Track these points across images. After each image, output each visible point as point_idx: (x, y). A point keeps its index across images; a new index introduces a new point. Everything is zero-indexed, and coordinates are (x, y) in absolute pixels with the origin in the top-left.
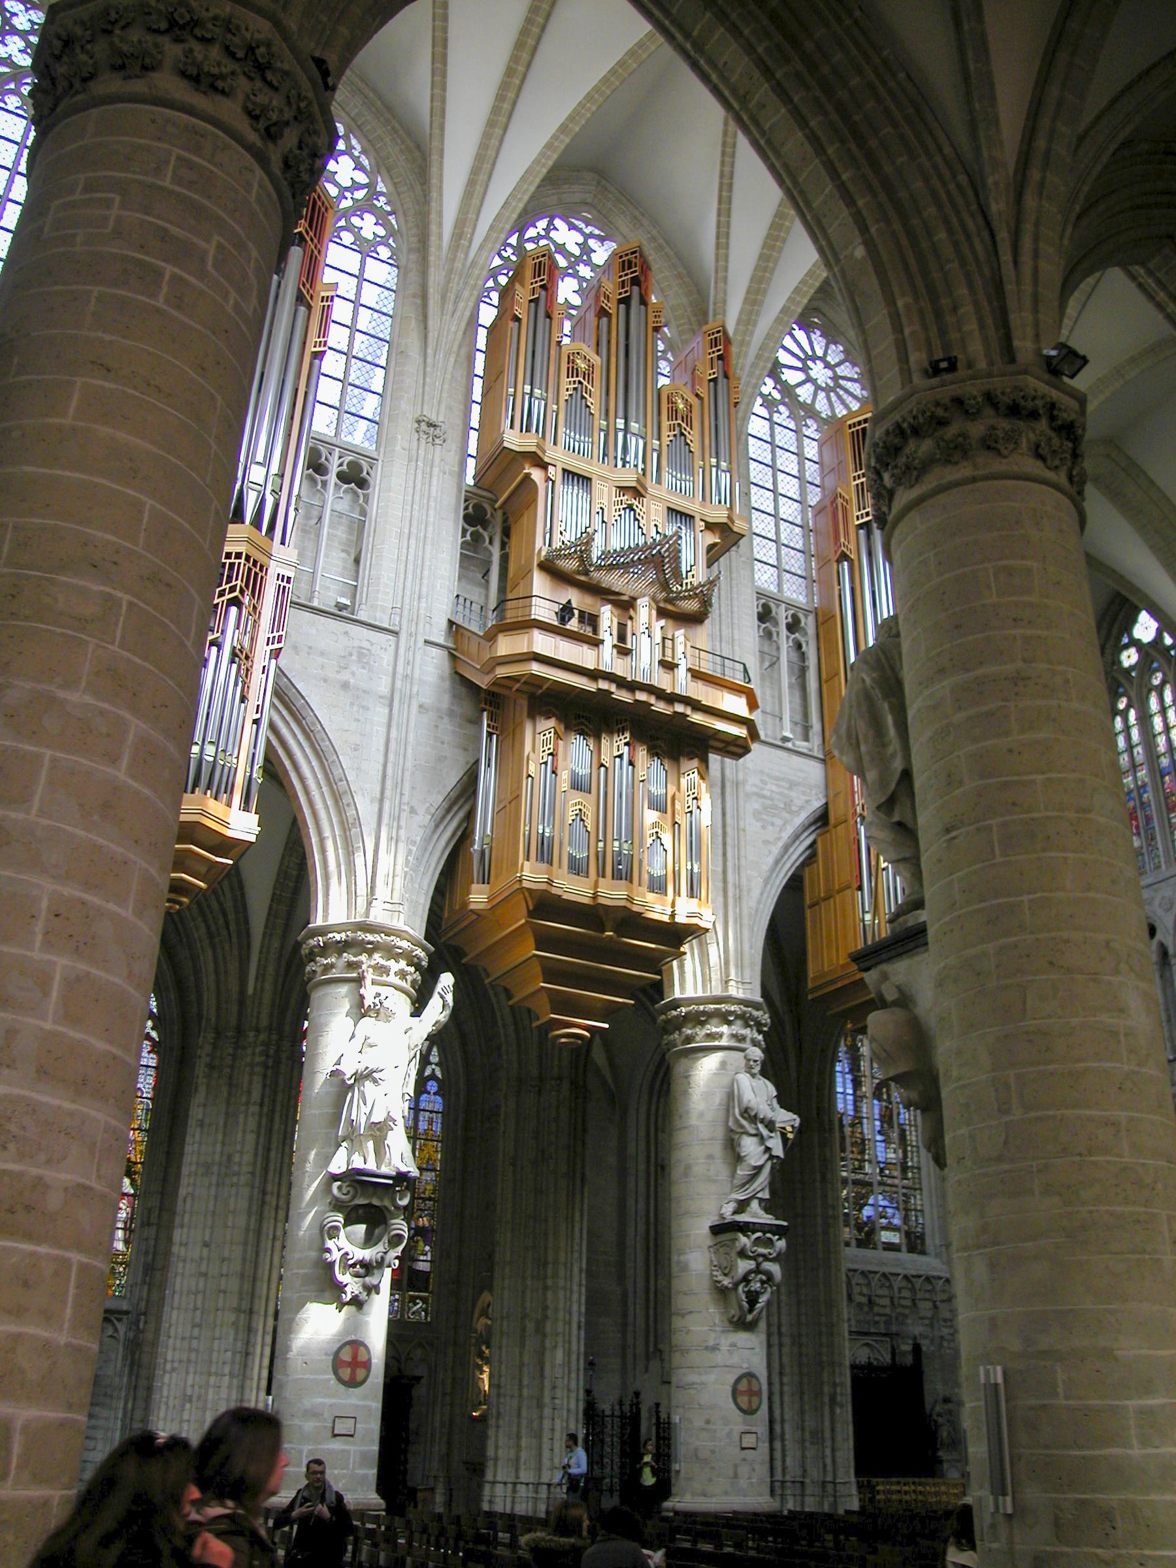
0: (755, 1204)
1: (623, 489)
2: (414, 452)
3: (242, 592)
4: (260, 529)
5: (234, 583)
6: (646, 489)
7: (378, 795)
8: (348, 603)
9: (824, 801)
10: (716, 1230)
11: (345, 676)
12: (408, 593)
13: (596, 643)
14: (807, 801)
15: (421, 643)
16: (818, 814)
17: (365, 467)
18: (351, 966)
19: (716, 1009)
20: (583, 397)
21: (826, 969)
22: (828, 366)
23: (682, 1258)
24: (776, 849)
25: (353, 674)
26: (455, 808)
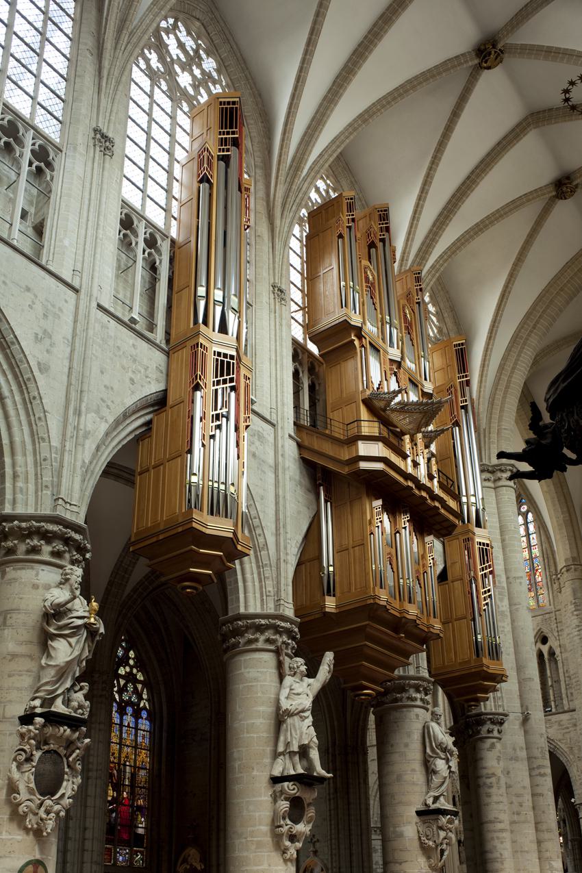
0: (442, 799)
10: (419, 813)
18: (268, 641)
19: (415, 684)
21: (446, 664)
23: (397, 829)
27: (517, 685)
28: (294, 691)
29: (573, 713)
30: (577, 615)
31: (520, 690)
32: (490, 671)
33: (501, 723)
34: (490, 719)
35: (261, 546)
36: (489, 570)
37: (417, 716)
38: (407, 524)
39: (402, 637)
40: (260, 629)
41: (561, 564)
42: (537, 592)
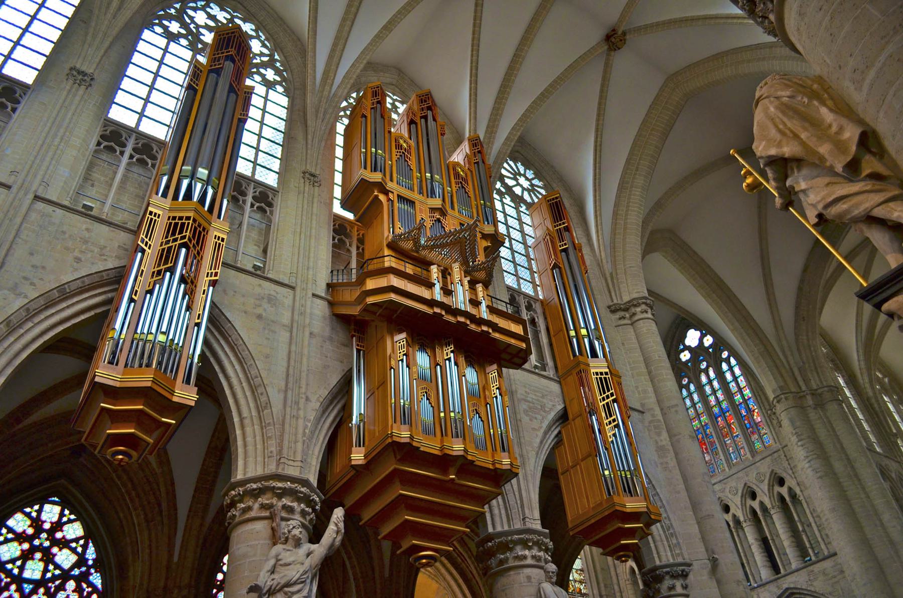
1: (433, 210)
2: (302, 189)
3: (190, 240)
4: (203, 205)
5: (184, 234)
6: (447, 211)
7: (283, 388)
8: (262, 266)
9: (563, 406)
11: (259, 311)
12: (301, 265)
13: (430, 286)
14: (553, 406)
15: (310, 295)
16: (561, 413)
17: (271, 196)
18: (263, 507)
20: (406, 161)
22: (527, 179)
24: (540, 433)
25: (265, 310)
26: (335, 402)
27: (696, 526)
28: (281, 562)
29: (836, 557)
30: (802, 446)
31: (701, 532)
32: (628, 510)
33: (684, 575)
34: (667, 573)
35: (263, 405)
36: (611, 399)
37: (529, 578)
38: (452, 355)
39: (453, 479)
40: (256, 494)
41: (771, 396)
42: (760, 433)
